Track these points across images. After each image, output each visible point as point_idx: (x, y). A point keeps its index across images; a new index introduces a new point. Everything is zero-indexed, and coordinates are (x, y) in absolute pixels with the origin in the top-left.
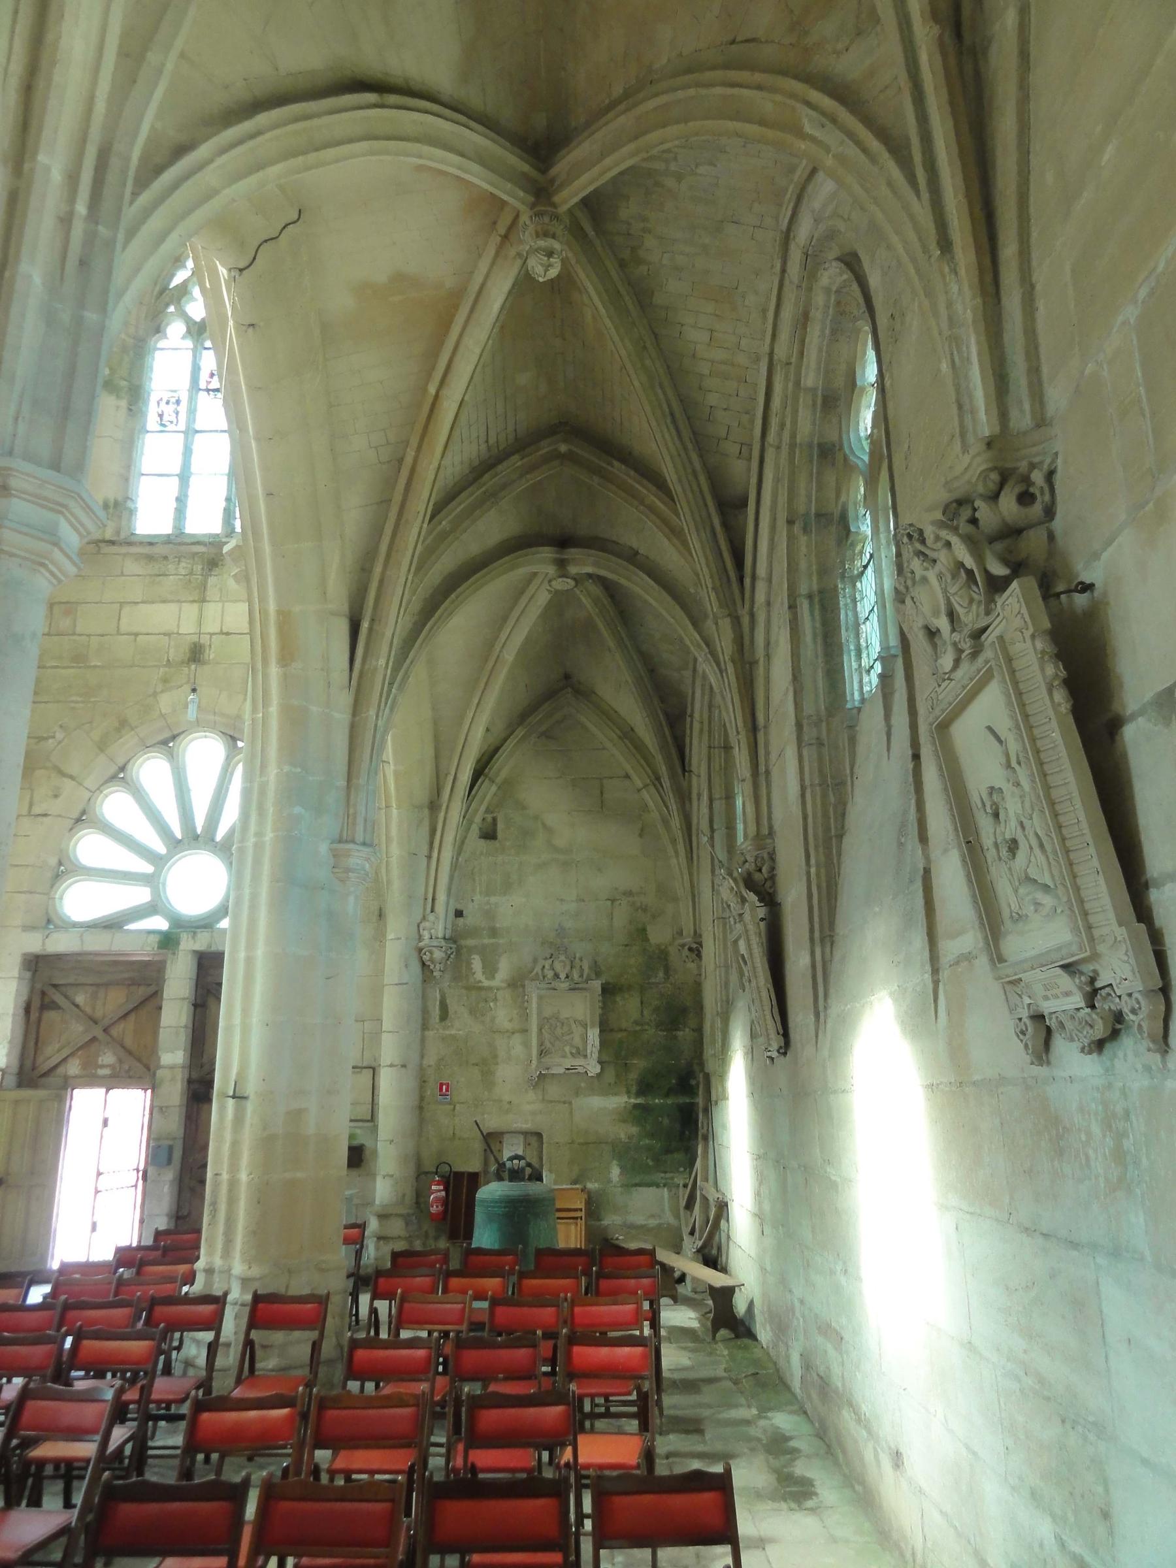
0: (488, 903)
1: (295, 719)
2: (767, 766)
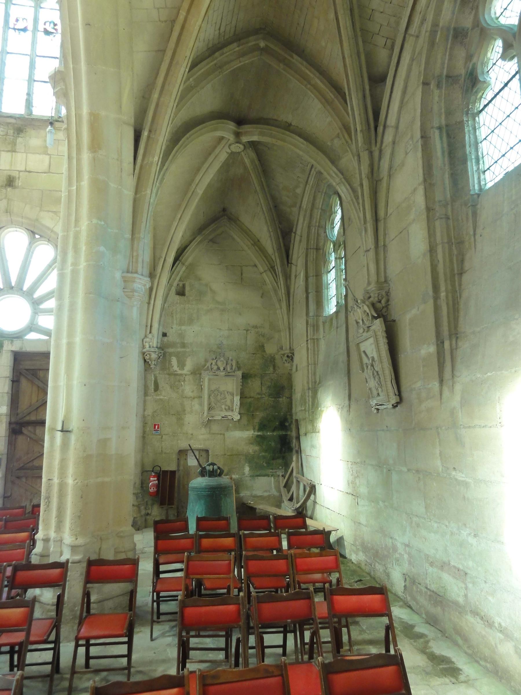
0: (180, 330)
1: (99, 188)
2: (384, 242)
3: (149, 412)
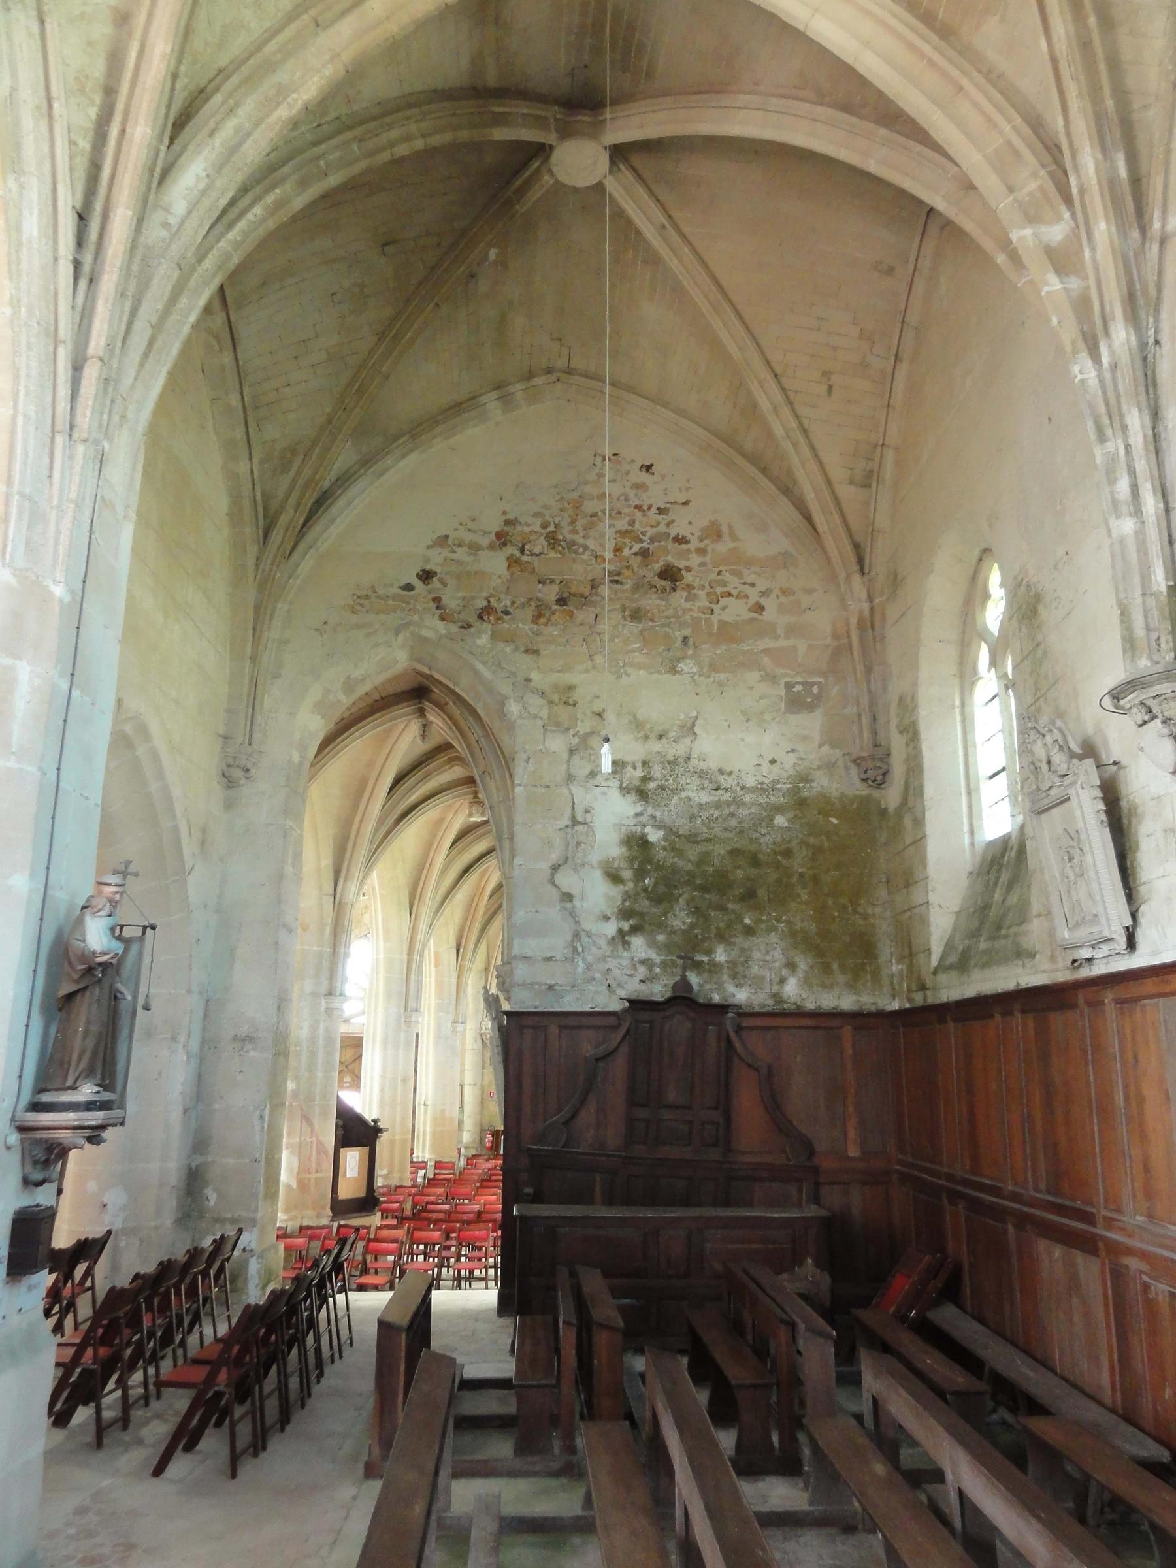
3: (486, 1082)
